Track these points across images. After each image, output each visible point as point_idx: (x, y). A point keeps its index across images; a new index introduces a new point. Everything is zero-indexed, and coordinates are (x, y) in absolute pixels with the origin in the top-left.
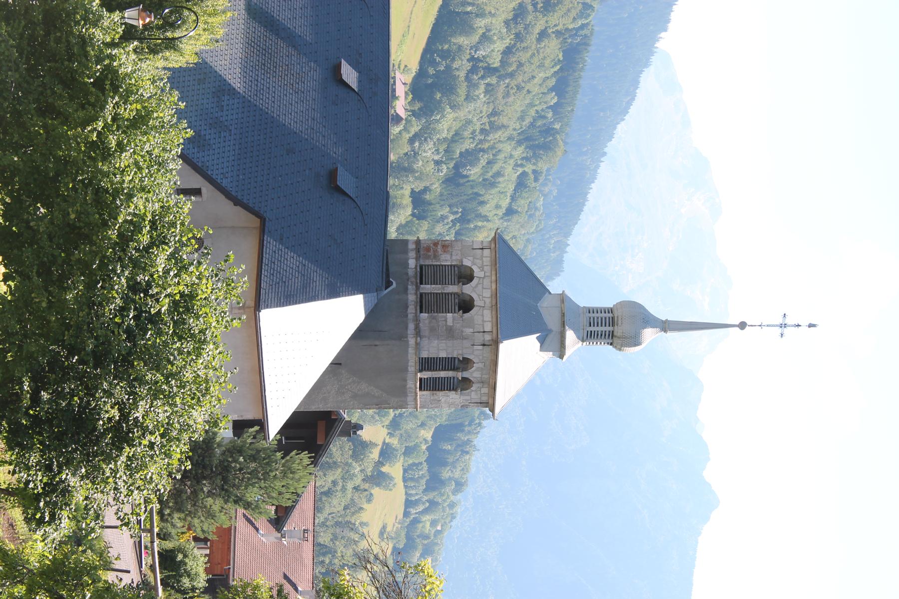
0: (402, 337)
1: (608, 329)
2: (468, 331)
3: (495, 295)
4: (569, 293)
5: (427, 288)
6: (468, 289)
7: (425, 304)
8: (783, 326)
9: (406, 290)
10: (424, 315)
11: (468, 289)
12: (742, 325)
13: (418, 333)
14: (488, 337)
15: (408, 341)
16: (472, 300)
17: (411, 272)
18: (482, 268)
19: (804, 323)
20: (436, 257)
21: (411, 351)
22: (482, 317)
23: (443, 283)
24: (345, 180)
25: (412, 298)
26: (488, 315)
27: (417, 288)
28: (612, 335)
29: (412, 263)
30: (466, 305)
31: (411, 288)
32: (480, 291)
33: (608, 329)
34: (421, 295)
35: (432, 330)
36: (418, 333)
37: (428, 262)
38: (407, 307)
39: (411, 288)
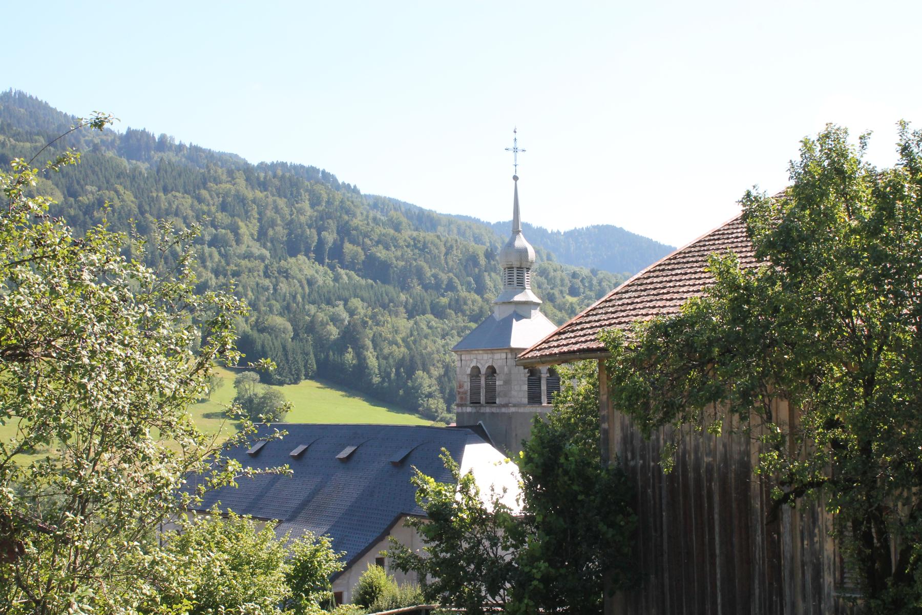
0: (510, 417)
1: (515, 272)
2: (506, 369)
3: (486, 351)
4: (133, 128)
5: (483, 399)
6: (483, 371)
7: (491, 402)
8: (515, 150)
9: (484, 414)
10: (497, 401)
11: (483, 371)
12: (516, 178)
13: (506, 405)
14: (509, 356)
15: (513, 413)
16: (489, 367)
17: (474, 410)
18: (471, 360)
19: (513, 136)
20: (465, 393)
21: (521, 410)
22: (499, 359)
23: (479, 388)
24: (397, 458)
25: (488, 410)
26: (497, 356)
27: (482, 406)
28: (520, 269)
29: (469, 409)
30: (492, 371)
31: (483, 410)
32: (483, 361)
33: (515, 272)
34: (487, 403)
35: (505, 395)
36: (506, 405)
37: (469, 398)
38: (493, 413)
39: (483, 410)
